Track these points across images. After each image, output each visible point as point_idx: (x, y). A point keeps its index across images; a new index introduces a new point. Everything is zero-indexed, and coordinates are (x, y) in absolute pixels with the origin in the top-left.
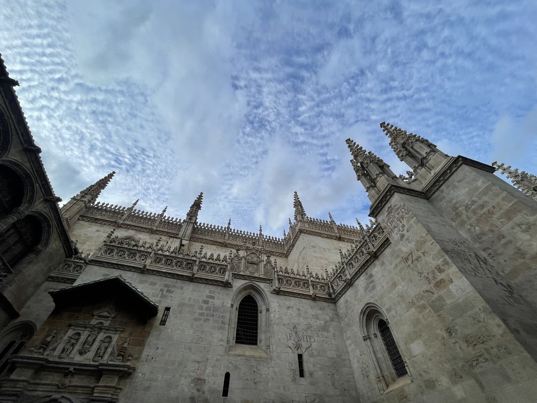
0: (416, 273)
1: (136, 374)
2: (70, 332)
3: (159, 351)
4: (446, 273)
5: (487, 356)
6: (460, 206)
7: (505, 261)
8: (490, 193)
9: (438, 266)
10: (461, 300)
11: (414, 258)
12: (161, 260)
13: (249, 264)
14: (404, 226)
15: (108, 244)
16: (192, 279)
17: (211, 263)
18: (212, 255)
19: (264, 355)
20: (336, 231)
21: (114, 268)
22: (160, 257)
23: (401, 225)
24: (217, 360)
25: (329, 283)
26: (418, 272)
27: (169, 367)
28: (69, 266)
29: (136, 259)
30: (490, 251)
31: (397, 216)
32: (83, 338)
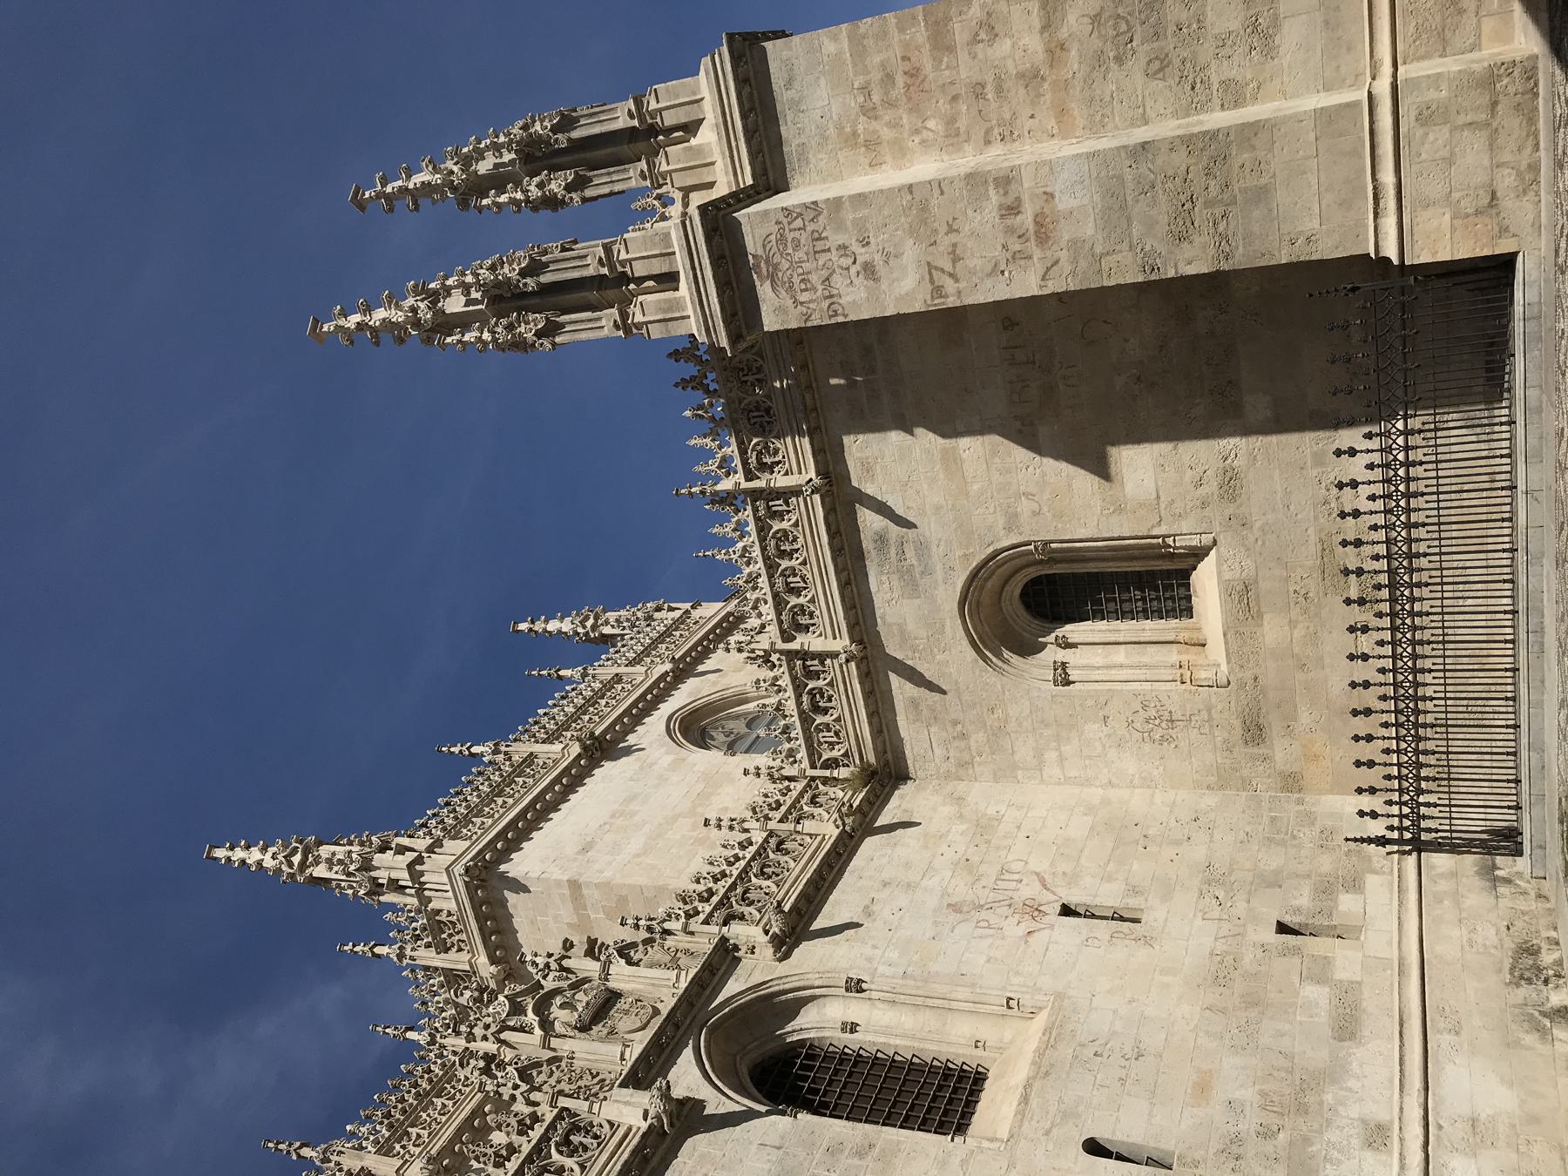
0: (989, 283)
4: (1026, 198)
5: (1218, 211)
6: (855, 123)
7: (1032, 117)
8: (869, 42)
9: (1001, 207)
10: (1097, 198)
11: (948, 267)
14: (843, 247)
19: (1041, 1020)
20: (557, 747)
23: (834, 255)
25: (810, 772)
26: (989, 275)
30: (996, 132)
31: (800, 254)
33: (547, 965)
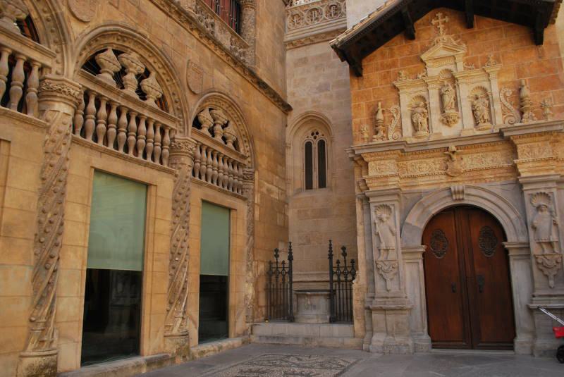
2: (407, 99)
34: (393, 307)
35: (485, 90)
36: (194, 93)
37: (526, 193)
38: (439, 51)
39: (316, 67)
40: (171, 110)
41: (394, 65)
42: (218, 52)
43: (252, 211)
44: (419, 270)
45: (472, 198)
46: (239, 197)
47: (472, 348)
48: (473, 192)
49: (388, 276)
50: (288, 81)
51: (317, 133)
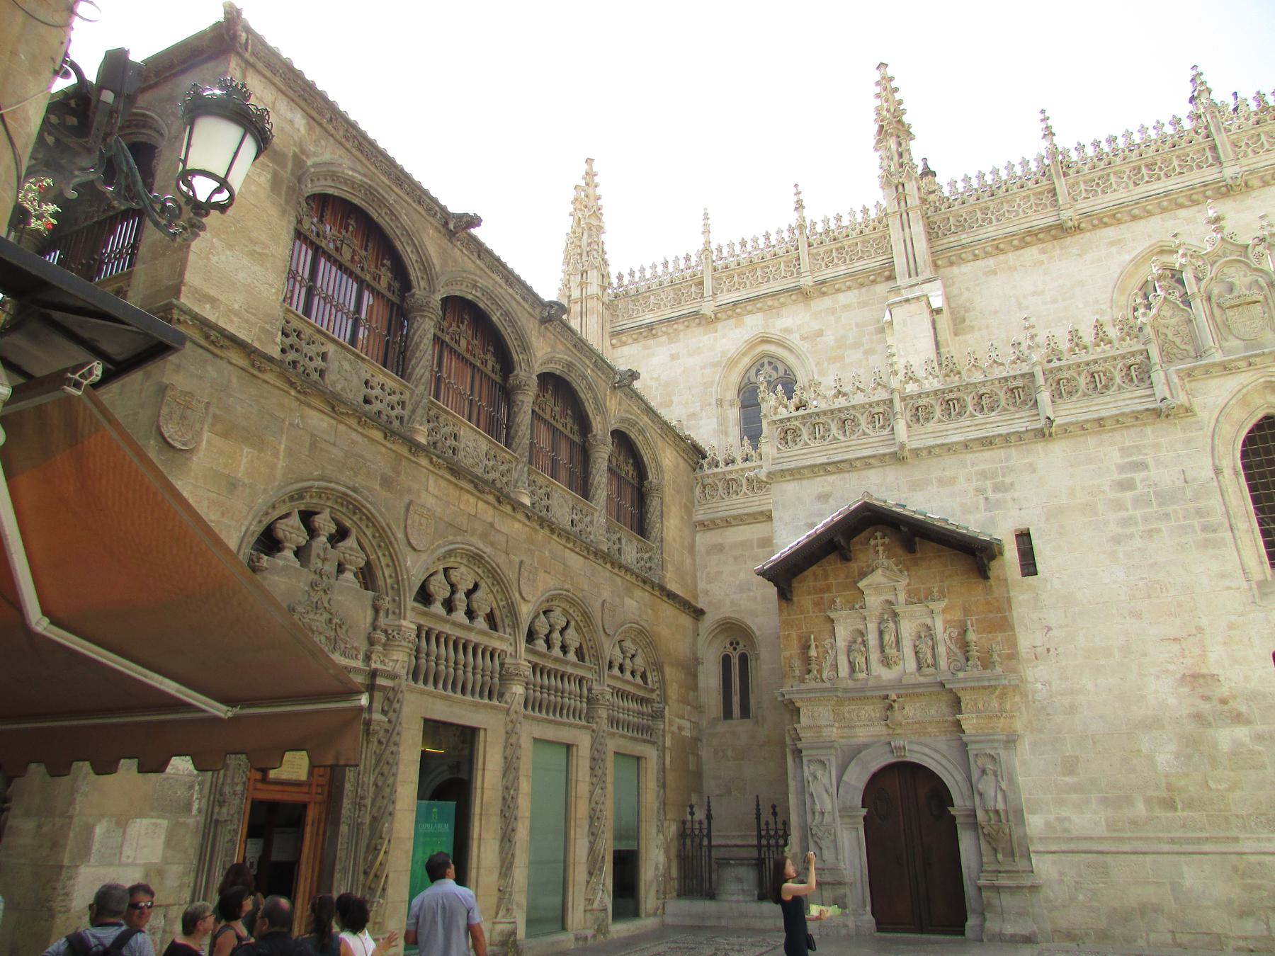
1: (1029, 686)
3: (1054, 633)
12: (929, 410)
13: (1229, 313)
15: (775, 418)
16: (1044, 434)
17: (1088, 364)
18: (1074, 335)
21: (828, 473)
22: (921, 402)
24: (1231, 627)
27: (1102, 663)
28: (714, 488)
29: (864, 434)
32: (872, 638)
33: (1262, 240)
34: (830, 880)
35: (929, 628)
36: (607, 635)
37: (971, 754)
38: (877, 577)
39: (736, 559)
40: (587, 657)
41: (828, 589)
42: (628, 577)
43: (662, 758)
44: (858, 837)
45: (915, 755)
46: (649, 742)
47: (922, 932)
48: (916, 748)
49: (825, 844)
50: (699, 574)
51: (738, 643)
